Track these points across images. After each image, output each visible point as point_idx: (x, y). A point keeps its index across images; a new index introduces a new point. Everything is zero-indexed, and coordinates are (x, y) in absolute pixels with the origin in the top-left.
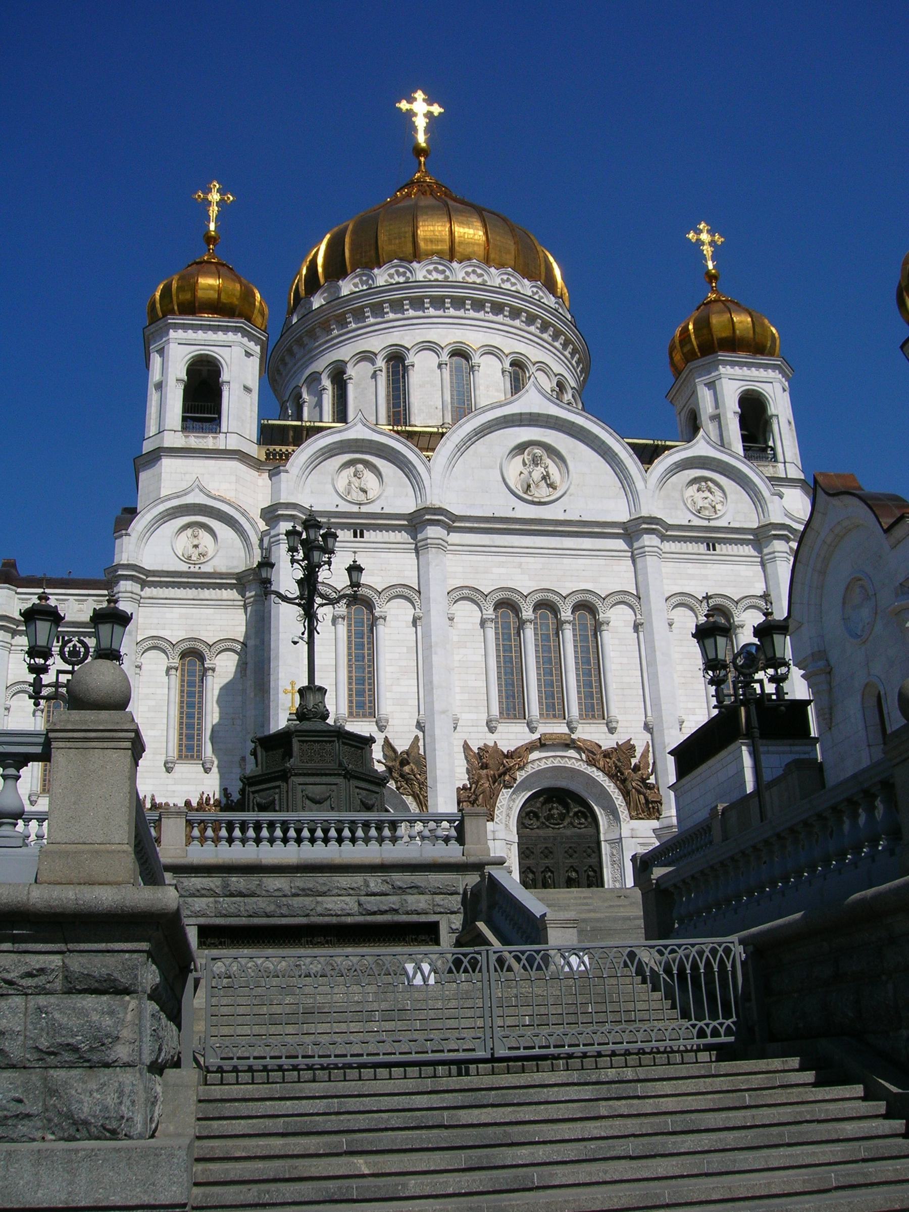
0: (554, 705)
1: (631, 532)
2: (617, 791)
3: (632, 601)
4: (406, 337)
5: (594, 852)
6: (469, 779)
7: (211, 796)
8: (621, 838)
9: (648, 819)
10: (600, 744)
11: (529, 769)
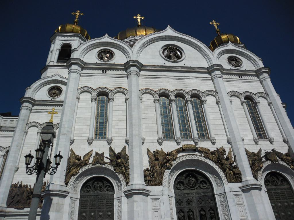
0: (186, 133)
1: (210, 70)
2: (220, 169)
3: (214, 94)
5: (212, 200)
6: (150, 166)
7: (46, 182)
8: (225, 193)
9: (236, 182)
10: (209, 149)
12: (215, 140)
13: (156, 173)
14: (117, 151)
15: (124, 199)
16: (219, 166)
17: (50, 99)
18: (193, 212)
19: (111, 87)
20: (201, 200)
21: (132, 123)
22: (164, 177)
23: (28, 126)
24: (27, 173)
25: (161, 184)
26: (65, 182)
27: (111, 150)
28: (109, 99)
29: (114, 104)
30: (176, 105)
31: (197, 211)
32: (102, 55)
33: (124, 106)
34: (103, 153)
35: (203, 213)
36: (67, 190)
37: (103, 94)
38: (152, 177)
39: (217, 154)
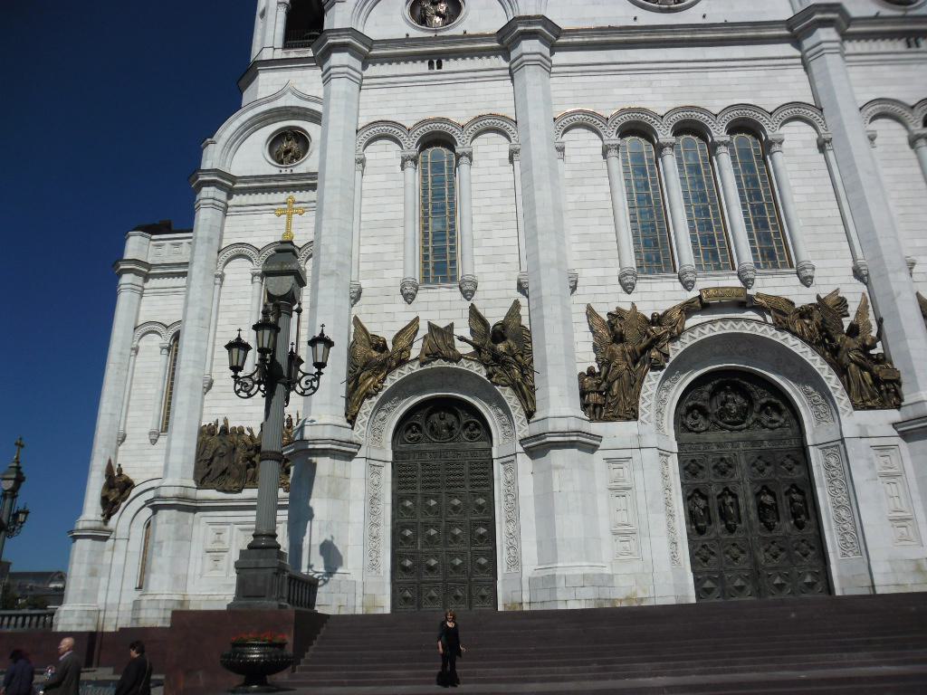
0: (713, 249)
2: (827, 366)
5: (797, 463)
6: (597, 360)
7: (294, 417)
8: (842, 440)
10: (791, 298)
11: (687, 341)
13: (616, 383)
14: (494, 316)
15: (524, 462)
16: (823, 356)
17: (275, 171)
18: (735, 496)
19: (460, 115)
20: (761, 463)
21: (534, 227)
22: (642, 394)
23: (223, 258)
24: (237, 392)
26: (346, 415)
27: (475, 314)
28: (458, 157)
29: (473, 171)
30: (679, 160)
31: (749, 493)
32: (424, 10)
33: (506, 175)
34: (452, 324)
35: (768, 499)
36: (354, 439)
37: (438, 143)
38: (607, 395)
39: (817, 316)
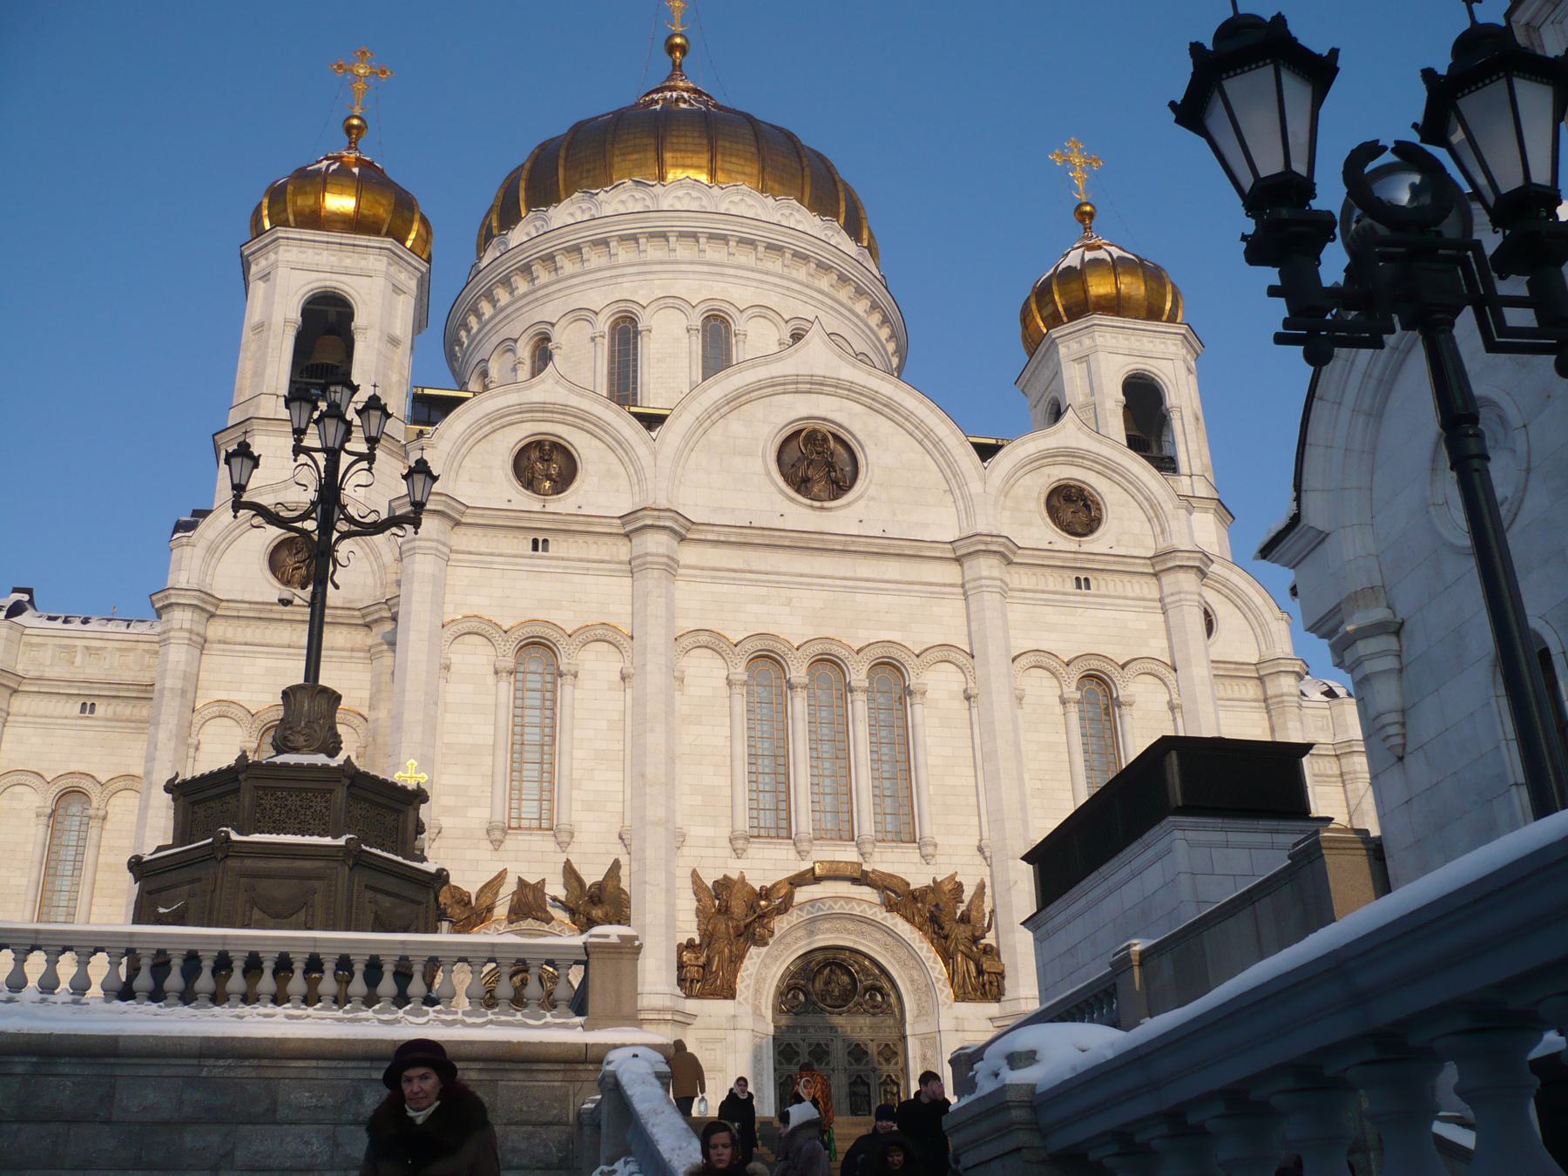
3: (962, 659)
4: (637, 290)
12: (935, 846)
14: (592, 874)
19: (568, 620)
21: (643, 776)
25: (729, 993)
27: (570, 872)
29: (578, 694)
37: (538, 648)
